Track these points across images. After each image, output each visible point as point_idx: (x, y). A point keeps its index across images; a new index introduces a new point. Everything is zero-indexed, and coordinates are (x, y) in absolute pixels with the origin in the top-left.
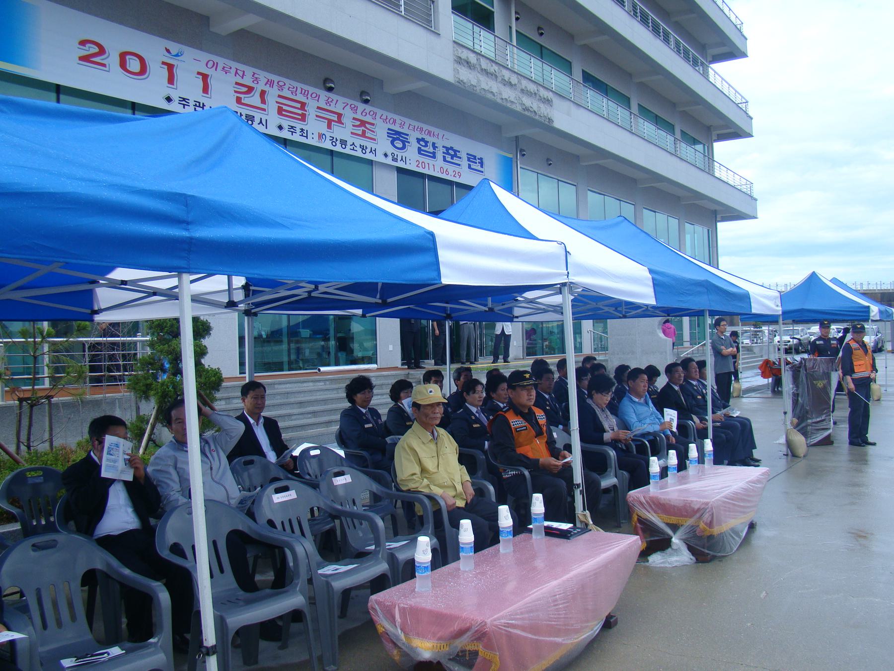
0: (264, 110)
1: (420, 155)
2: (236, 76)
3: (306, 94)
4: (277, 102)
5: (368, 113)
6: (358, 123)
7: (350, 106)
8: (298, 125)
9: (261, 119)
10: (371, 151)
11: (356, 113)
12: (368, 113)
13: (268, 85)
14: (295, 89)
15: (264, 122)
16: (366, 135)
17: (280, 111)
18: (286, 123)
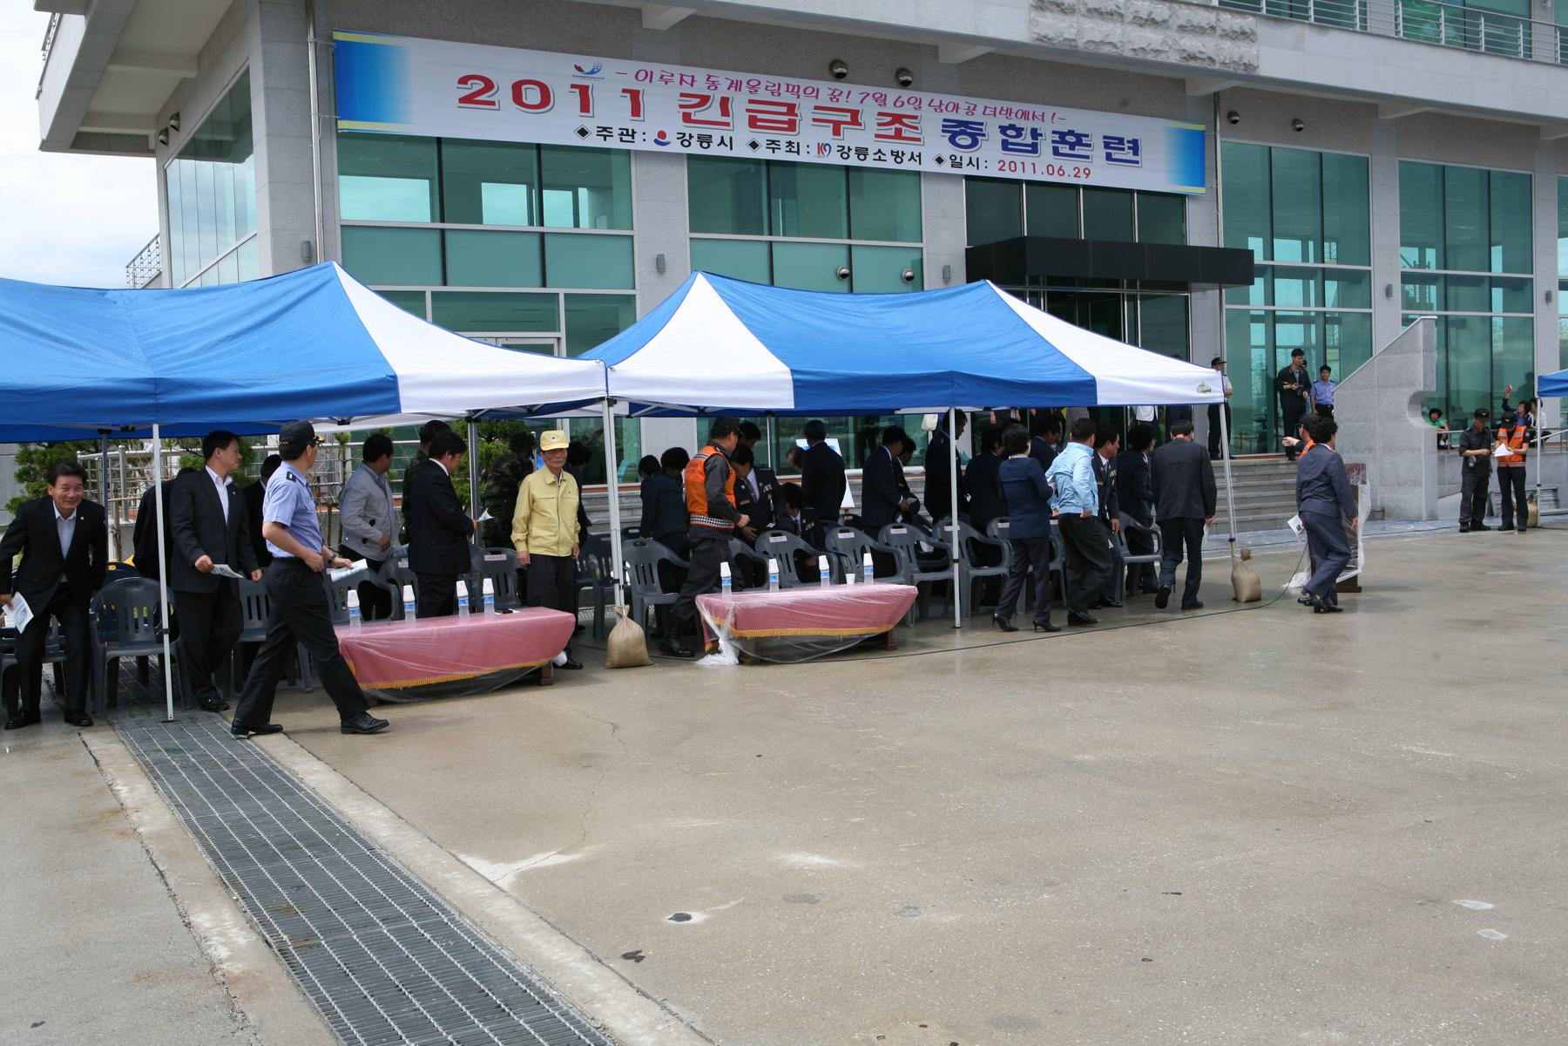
0: (728, 124)
1: (1006, 152)
2: (681, 84)
3: (796, 90)
4: (748, 110)
5: (906, 102)
6: (888, 119)
7: (873, 96)
8: (783, 138)
9: (722, 137)
10: (912, 157)
11: (885, 104)
12: (906, 102)
13: (733, 89)
14: (776, 87)
15: (727, 141)
16: (903, 135)
17: (753, 122)
18: (762, 137)
